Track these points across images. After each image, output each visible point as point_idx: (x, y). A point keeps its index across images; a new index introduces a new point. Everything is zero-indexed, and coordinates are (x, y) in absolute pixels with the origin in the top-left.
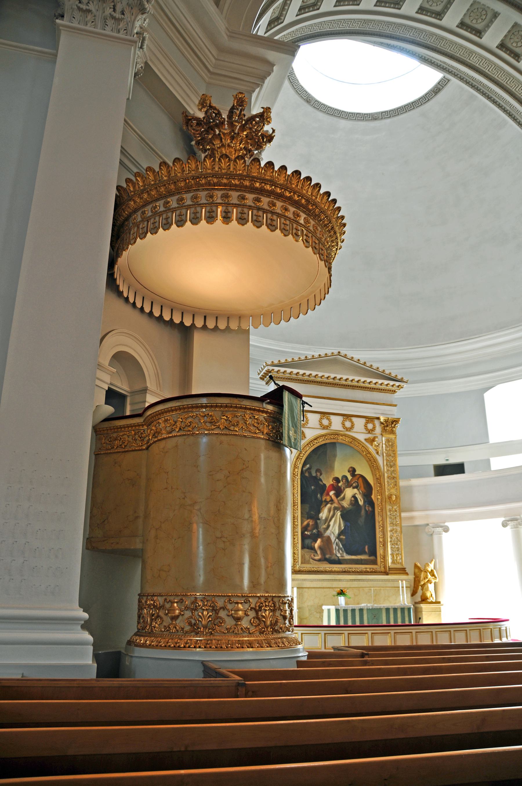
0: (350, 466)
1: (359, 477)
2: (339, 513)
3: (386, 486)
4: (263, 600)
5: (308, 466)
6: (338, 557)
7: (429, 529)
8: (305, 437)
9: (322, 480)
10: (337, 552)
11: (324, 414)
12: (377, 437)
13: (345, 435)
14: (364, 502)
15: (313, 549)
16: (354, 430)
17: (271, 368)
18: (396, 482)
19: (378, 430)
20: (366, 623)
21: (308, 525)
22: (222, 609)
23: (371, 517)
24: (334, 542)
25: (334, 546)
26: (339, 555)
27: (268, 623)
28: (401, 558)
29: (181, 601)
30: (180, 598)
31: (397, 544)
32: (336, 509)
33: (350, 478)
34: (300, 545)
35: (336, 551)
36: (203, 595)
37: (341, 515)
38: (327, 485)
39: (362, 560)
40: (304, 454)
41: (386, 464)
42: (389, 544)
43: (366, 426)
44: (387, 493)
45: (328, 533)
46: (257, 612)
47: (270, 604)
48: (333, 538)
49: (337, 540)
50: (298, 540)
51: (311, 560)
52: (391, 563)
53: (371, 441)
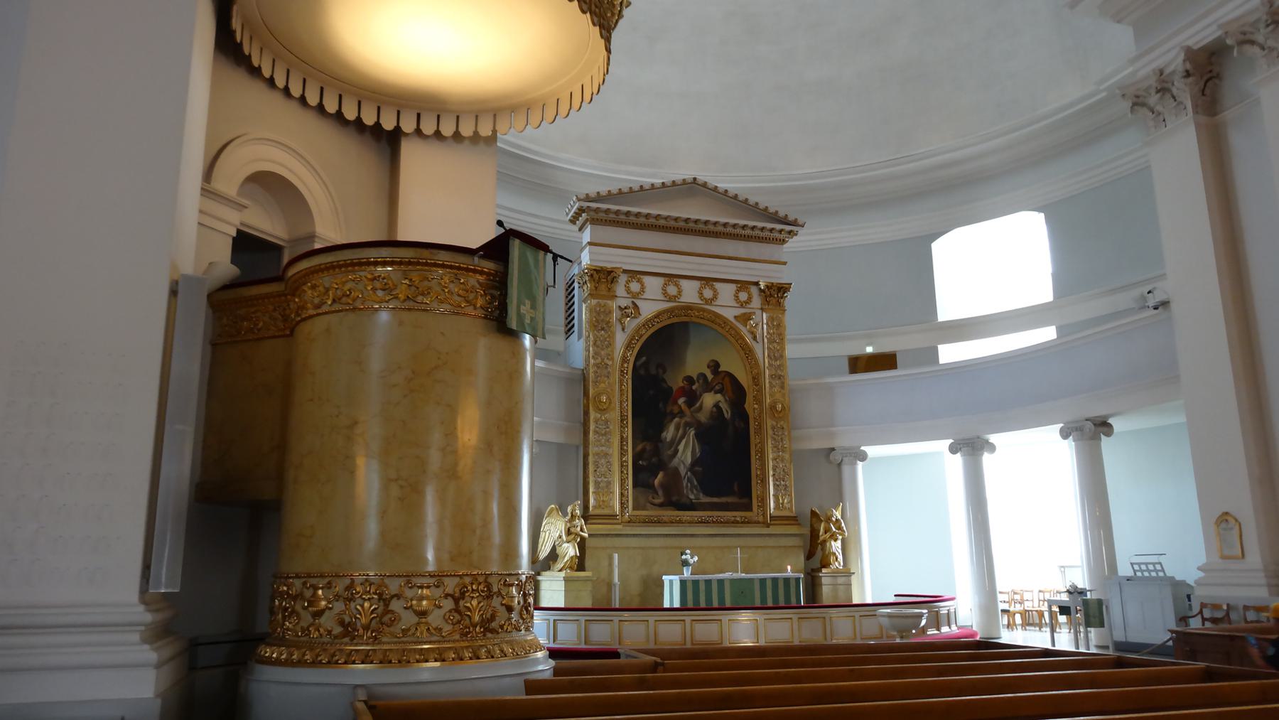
0: (711, 359)
1: (725, 376)
2: (692, 433)
3: (767, 389)
4: (467, 580)
5: (644, 358)
6: (691, 500)
7: (835, 457)
8: (639, 313)
9: (666, 379)
10: (690, 492)
11: (670, 278)
12: (754, 313)
13: (704, 310)
15: (651, 487)
17: (586, 204)
18: (783, 383)
19: (756, 302)
20: (728, 604)
21: (643, 450)
22: (395, 598)
24: (685, 477)
26: (692, 497)
27: (477, 618)
28: (790, 502)
29: (329, 586)
30: (327, 580)
32: (688, 425)
33: (710, 376)
35: (687, 491)
36: (364, 575)
37: (695, 434)
38: (675, 388)
39: (727, 503)
40: (638, 340)
41: (768, 356)
42: (771, 479)
43: (737, 297)
44: (768, 401)
45: (675, 461)
46: (456, 601)
47: (481, 587)
48: (683, 471)
49: (689, 473)
50: (627, 474)
51: (648, 505)
52: (774, 509)
53: (745, 318)
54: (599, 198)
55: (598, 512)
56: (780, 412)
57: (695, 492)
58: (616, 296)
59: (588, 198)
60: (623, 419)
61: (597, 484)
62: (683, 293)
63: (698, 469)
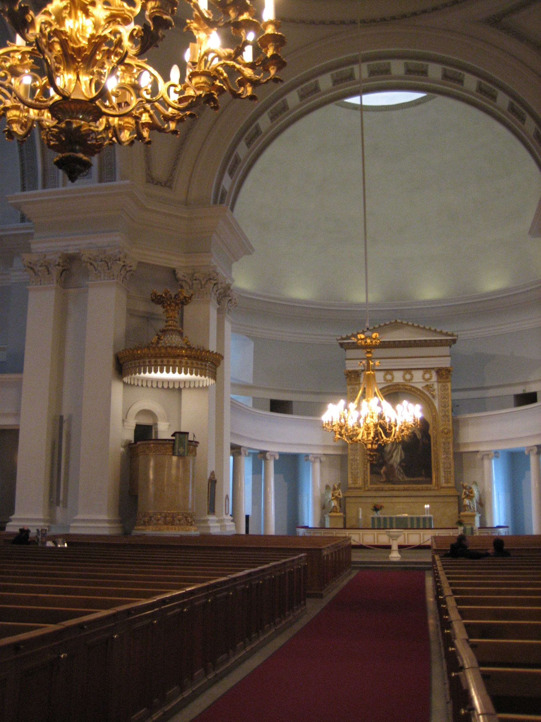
2: (400, 447)
11: (388, 371)
12: (433, 385)
14: (422, 437)
15: (378, 473)
16: (414, 381)
19: (434, 378)
23: (427, 448)
25: (396, 471)
26: (400, 478)
31: (449, 469)
45: (391, 461)
48: (395, 466)
49: (399, 467)
55: (353, 486)
56: (447, 433)
57: (402, 475)
59: (342, 339)
62: (395, 378)
63: (403, 464)
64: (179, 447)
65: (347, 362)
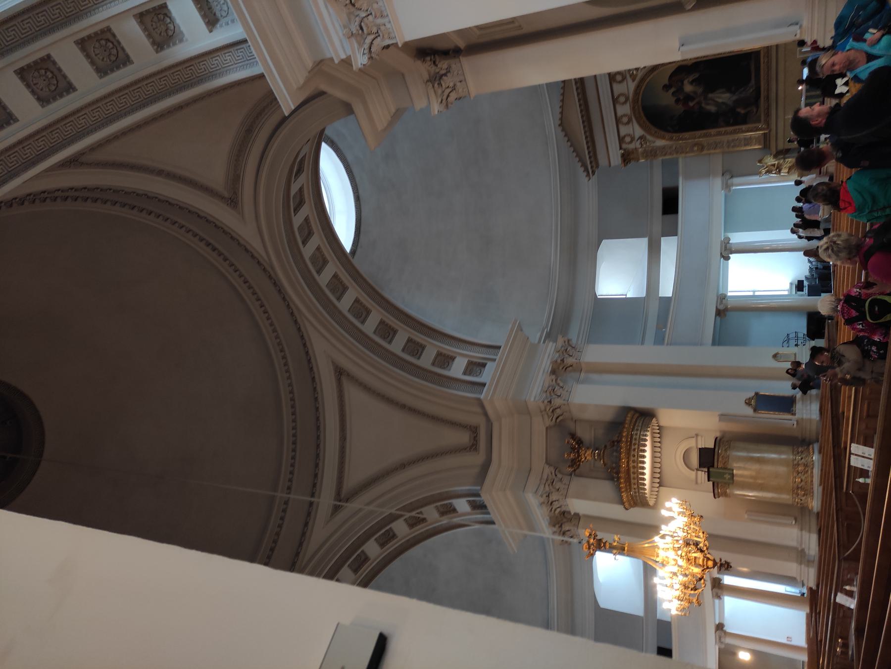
2: (710, 95)
8: (643, 135)
11: (618, 121)
26: (751, 90)
34: (744, 127)
43: (620, 82)
48: (735, 98)
54: (586, 170)
58: (636, 148)
59: (588, 175)
60: (705, 136)
61: (745, 145)
64: (725, 478)
65: (612, 164)
